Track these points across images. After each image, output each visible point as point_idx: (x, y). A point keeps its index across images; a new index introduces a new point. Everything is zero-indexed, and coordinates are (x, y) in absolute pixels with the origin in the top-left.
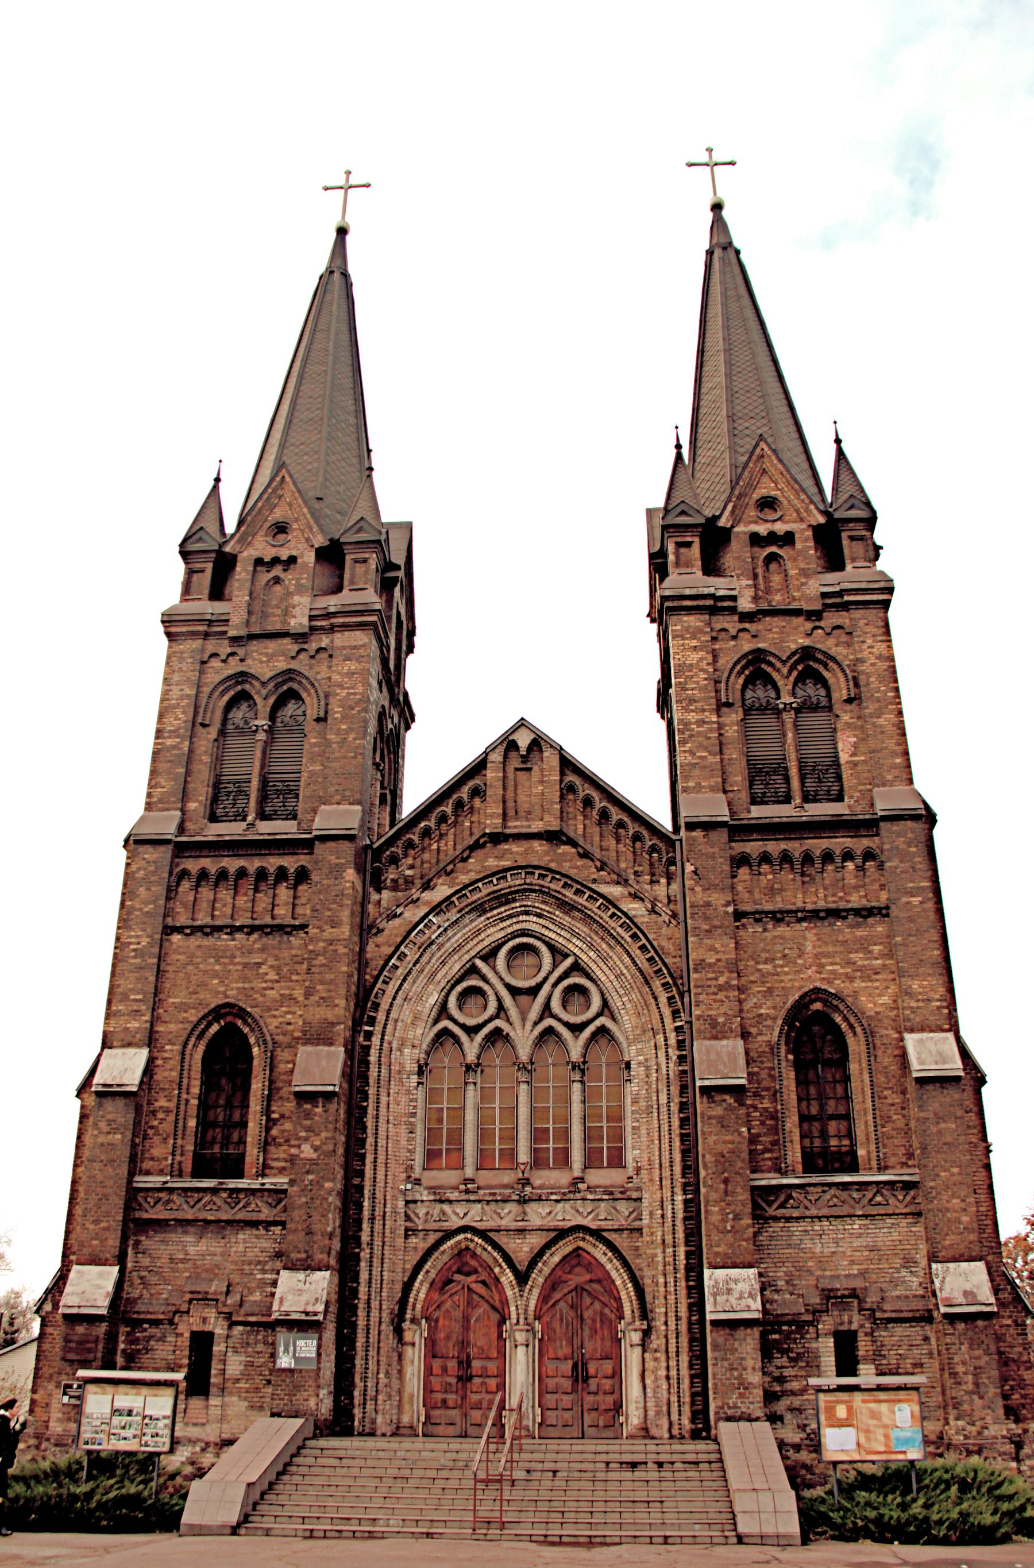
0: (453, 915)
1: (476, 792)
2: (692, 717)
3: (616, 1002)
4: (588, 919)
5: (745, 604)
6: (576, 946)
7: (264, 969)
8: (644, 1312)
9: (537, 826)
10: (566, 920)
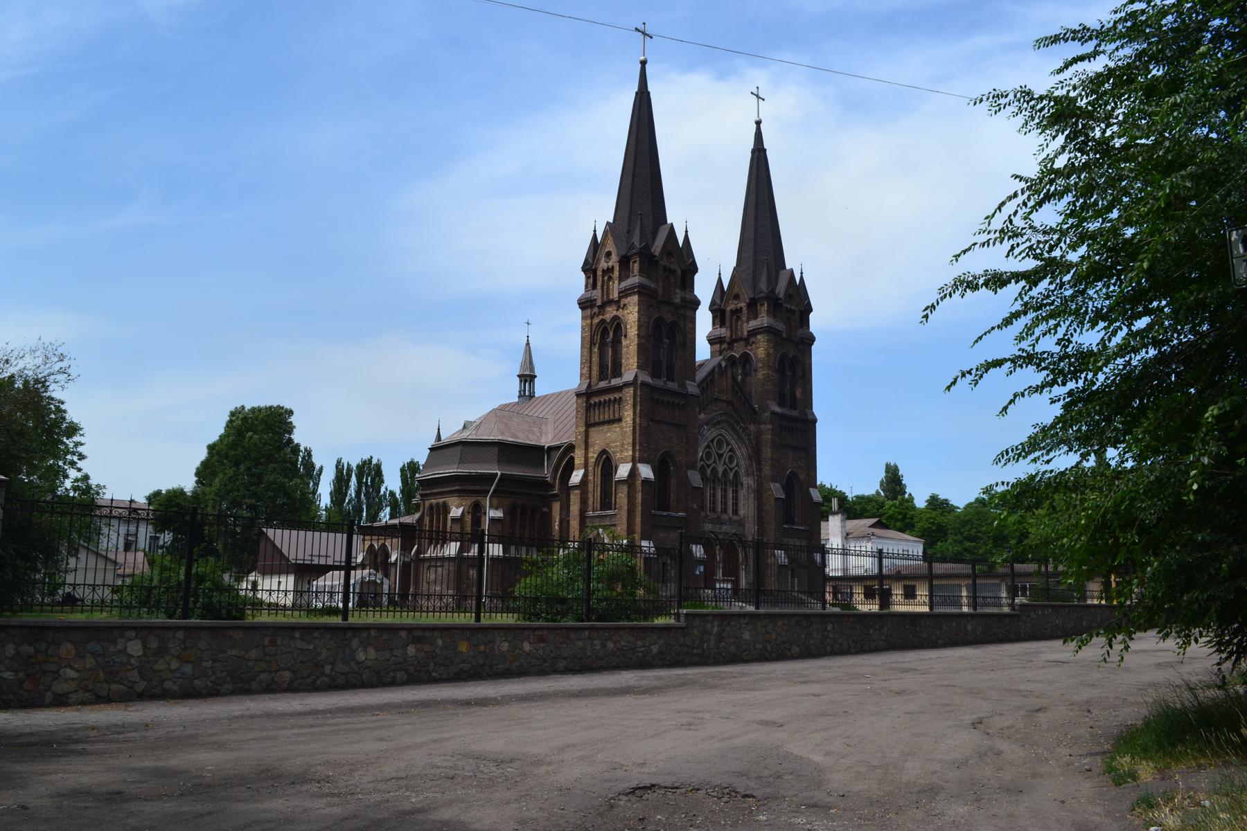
0: (709, 426)
1: (711, 380)
2: (770, 373)
3: (742, 463)
4: (738, 434)
5: (784, 335)
6: (733, 442)
7: (674, 439)
8: (747, 560)
9: (724, 398)
10: (732, 433)
